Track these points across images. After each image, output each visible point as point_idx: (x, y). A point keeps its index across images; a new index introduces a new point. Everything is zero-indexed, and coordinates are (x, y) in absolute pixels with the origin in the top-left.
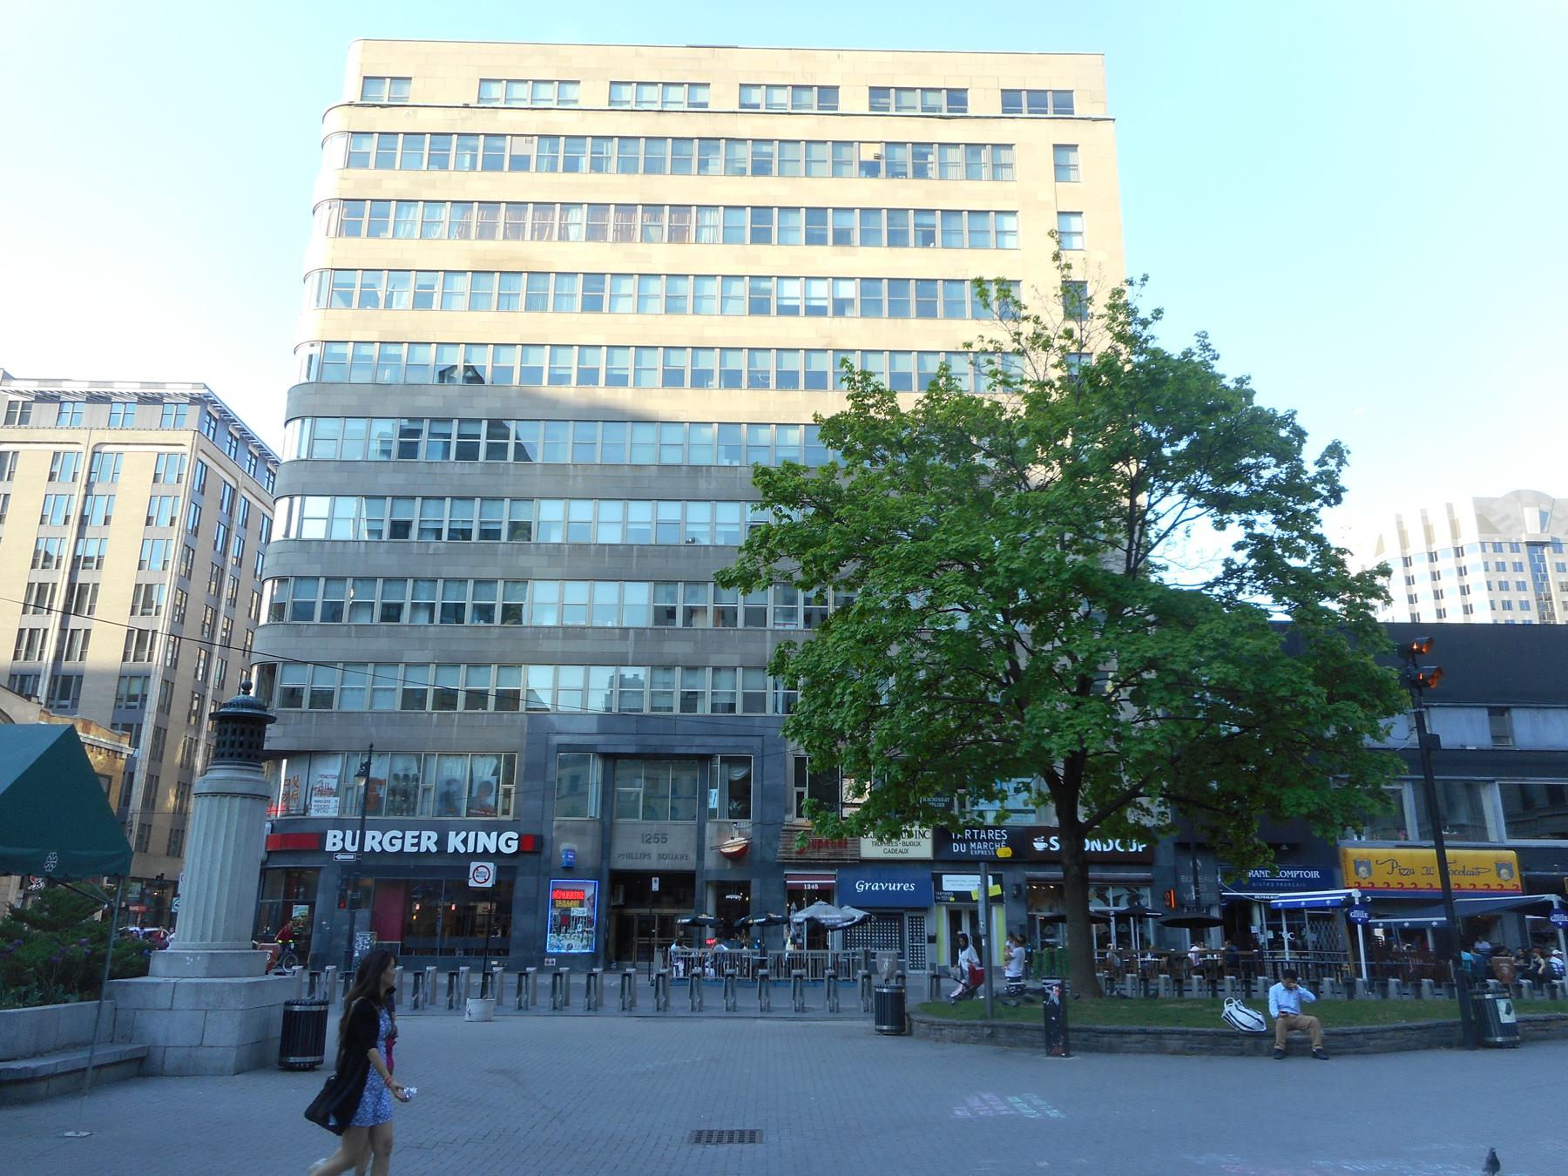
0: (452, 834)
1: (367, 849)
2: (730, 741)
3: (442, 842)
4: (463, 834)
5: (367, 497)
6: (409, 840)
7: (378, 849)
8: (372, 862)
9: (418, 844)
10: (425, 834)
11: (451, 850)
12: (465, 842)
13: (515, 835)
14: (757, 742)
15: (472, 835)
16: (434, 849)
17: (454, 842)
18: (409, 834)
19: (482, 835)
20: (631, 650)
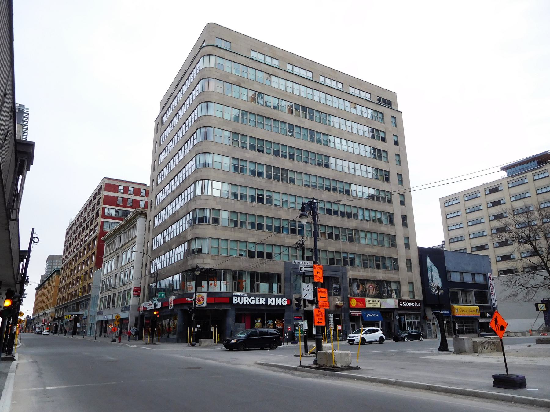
0: (269, 299)
1: (245, 303)
2: (335, 273)
3: (266, 301)
4: (272, 299)
5: (232, 184)
6: (257, 301)
7: (248, 303)
8: (244, 307)
9: (259, 302)
10: (261, 299)
11: (269, 304)
12: (273, 301)
13: (286, 300)
14: (340, 274)
15: (274, 299)
16: (264, 303)
17: (270, 301)
18: (257, 298)
19: (277, 299)
20: (309, 244)
